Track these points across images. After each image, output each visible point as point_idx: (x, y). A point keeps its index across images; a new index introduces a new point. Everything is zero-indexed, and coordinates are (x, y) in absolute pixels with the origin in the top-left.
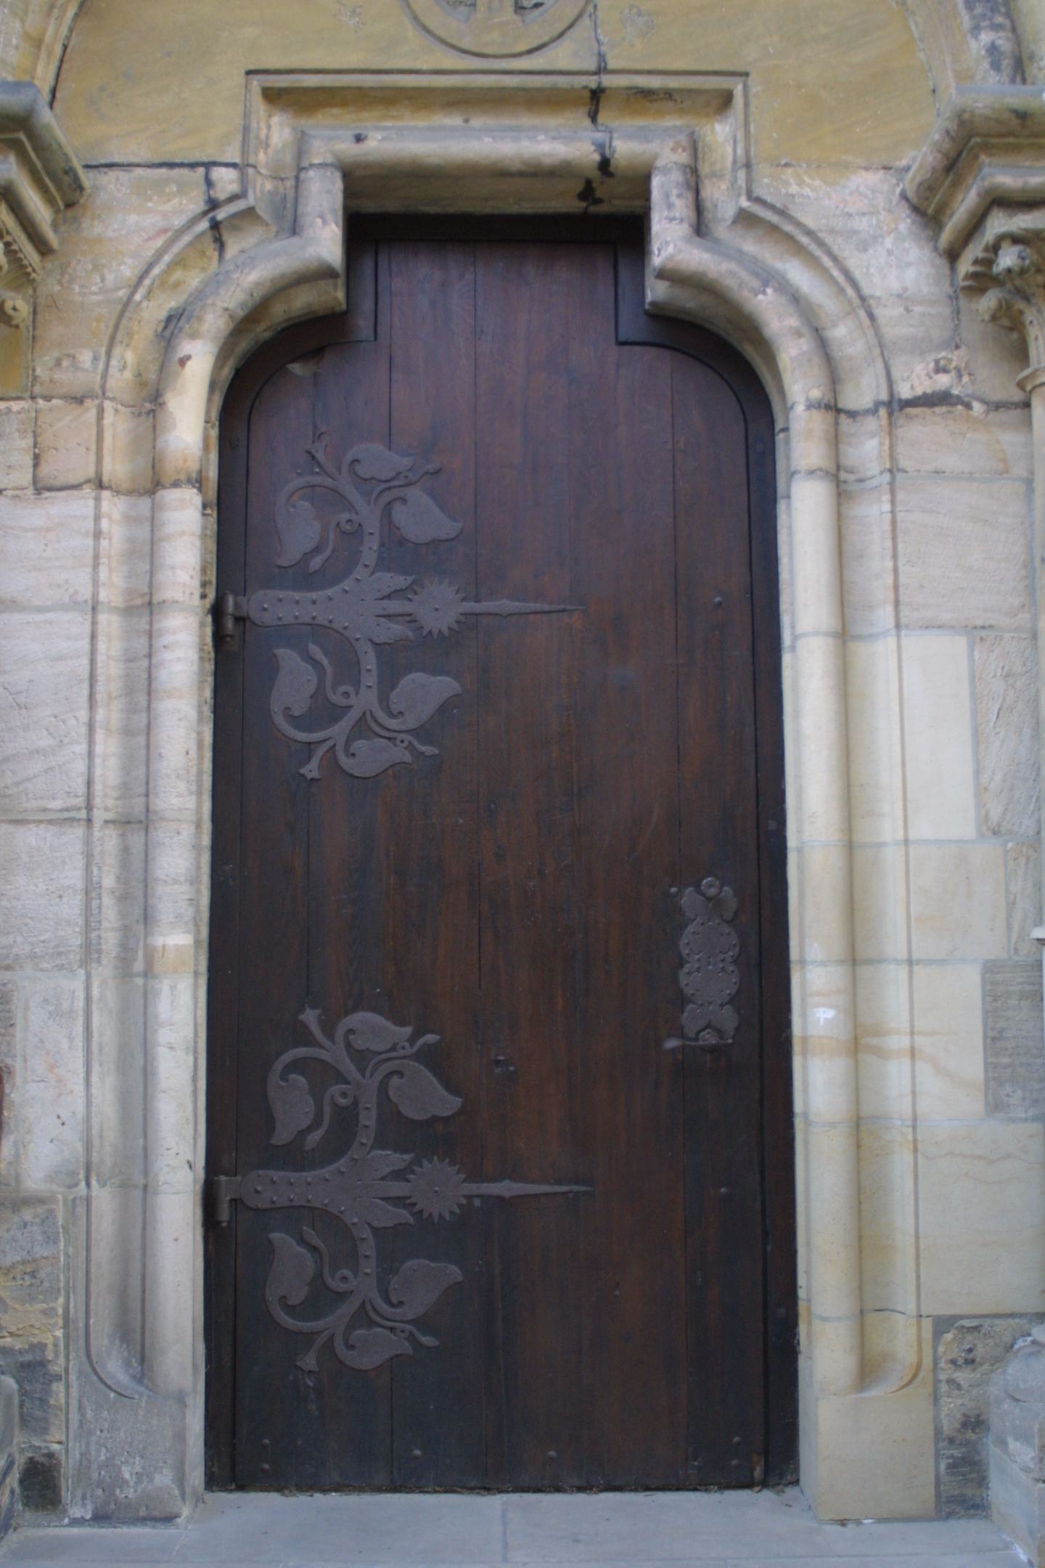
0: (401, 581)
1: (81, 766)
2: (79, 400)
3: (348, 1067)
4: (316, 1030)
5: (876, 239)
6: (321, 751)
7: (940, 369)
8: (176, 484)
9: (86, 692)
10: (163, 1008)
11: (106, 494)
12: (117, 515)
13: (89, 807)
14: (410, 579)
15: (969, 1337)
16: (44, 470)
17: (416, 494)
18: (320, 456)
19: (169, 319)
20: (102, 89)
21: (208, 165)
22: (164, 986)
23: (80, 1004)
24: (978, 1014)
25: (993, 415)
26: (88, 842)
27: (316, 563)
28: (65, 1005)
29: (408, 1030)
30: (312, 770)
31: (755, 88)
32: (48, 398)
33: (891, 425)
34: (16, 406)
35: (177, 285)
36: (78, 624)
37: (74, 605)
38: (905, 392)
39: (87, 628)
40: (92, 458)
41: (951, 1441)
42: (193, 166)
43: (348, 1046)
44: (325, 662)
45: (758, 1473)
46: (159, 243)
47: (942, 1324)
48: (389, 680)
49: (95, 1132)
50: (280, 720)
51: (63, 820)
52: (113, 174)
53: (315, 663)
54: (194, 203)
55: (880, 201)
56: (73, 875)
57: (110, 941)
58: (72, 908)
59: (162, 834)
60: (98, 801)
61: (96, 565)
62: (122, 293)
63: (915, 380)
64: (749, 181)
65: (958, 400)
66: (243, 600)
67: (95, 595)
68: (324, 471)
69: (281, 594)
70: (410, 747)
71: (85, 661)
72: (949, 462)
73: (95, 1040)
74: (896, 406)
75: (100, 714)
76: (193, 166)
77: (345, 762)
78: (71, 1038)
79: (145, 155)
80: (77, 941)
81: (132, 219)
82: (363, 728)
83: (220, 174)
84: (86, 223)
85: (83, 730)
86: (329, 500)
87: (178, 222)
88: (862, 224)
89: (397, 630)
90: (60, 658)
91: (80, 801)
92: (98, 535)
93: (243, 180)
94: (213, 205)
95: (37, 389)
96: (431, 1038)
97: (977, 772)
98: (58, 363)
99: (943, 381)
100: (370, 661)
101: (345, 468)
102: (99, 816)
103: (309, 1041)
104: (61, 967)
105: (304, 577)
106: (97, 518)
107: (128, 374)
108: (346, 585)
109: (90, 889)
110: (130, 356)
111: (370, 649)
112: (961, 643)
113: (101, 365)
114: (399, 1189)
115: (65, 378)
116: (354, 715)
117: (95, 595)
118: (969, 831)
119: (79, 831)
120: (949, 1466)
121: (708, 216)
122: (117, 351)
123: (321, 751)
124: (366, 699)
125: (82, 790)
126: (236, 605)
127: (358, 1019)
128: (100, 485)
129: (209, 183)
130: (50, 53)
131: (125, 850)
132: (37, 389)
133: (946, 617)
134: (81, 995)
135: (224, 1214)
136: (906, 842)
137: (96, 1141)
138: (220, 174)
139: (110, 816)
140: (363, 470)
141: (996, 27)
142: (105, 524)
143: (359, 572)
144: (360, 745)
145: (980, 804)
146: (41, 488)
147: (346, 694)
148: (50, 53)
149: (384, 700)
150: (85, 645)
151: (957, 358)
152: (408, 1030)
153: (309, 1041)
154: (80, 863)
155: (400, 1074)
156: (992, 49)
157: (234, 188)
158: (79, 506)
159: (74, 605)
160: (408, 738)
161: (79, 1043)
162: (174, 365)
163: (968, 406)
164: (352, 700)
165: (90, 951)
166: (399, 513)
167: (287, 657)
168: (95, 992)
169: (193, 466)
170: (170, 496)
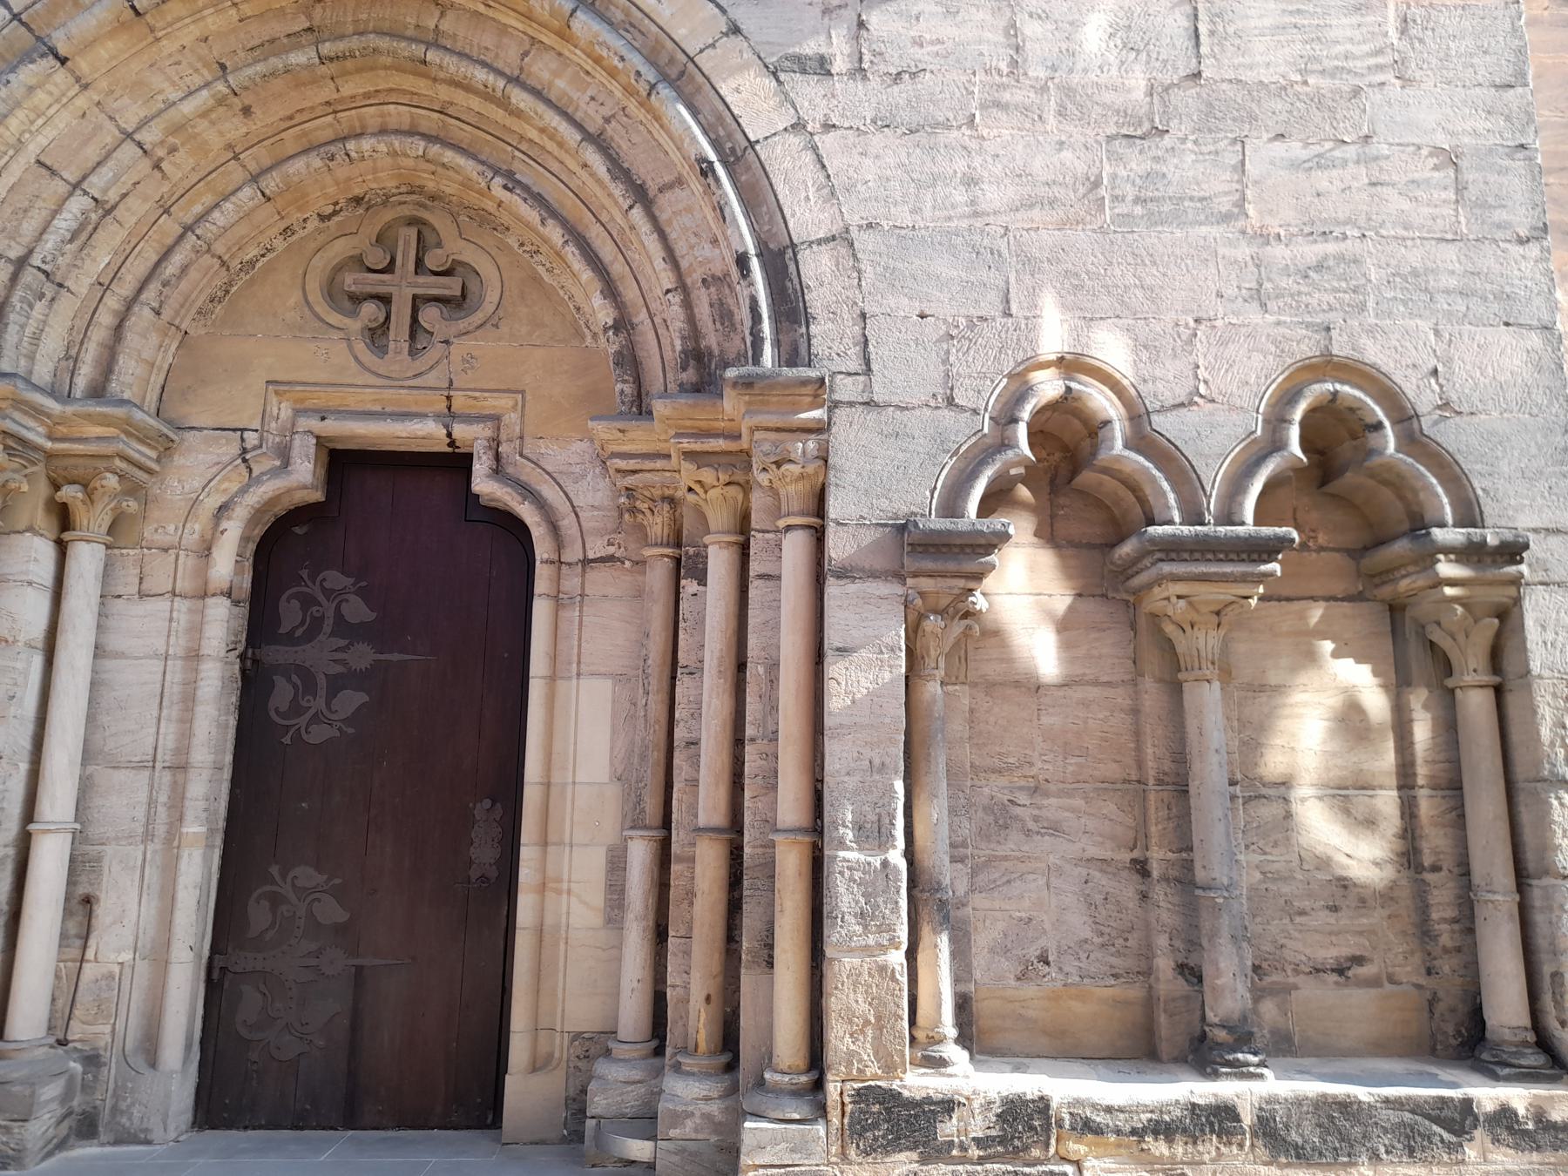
0: (343, 643)
1: (151, 740)
2: (166, 550)
3: (292, 897)
4: (277, 878)
5: (584, 476)
6: (293, 730)
7: (610, 544)
8: (213, 595)
9: (158, 701)
10: (183, 865)
11: (177, 599)
12: (184, 609)
13: (154, 761)
14: (347, 642)
15: (587, 1043)
16: (144, 586)
17: (352, 598)
18: (305, 576)
19: (220, 507)
20: (189, 387)
21: (243, 430)
22: (185, 854)
23: (139, 863)
24: (603, 873)
25: (636, 567)
26: (152, 779)
27: (299, 633)
28: (131, 864)
29: (325, 877)
30: (287, 740)
31: (528, 397)
32: (149, 549)
33: (584, 571)
34: (132, 552)
35: (225, 490)
36: (157, 666)
37: (156, 656)
38: (591, 555)
39: (162, 668)
40: (171, 580)
41: (574, 1100)
42: (234, 430)
43: (293, 885)
44: (299, 682)
45: (489, 1121)
46: (214, 470)
47: (577, 1036)
48: (332, 693)
49: (141, 931)
50: (273, 714)
51: (140, 766)
52: (193, 432)
53: (295, 686)
54: (235, 450)
55: (587, 457)
56: (143, 796)
57: (161, 830)
58: (140, 813)
59: (192, 774)
60: (159, 757)
61: (168, 636)
62: (194, 496)
63: (597, 549)
64: (522, 446)
65: (619, 559)
66: (257, 651)
67: (167, 651)
68: (306, 585)
69: (278, 647)
70: (340, 729)
71: (158, 686)
72: (611, 591)
73: (146, 882)
74: (586, 562)
75: (165, 712)
76: (234, 430)
77: (305, 736)
78: (133, 881)
79: (210, 424)
80: (140, 830)
81: (201, 456)
82: (316, 719)
83: (246, 434)
84: (176, 457)
85: (155, 721)
86: (307, 601)
87: (226, 459)
88: (577, 469)
89: (339, 669)
90: (145, 683)
91: (150, 758)
92: (171, 620)
93: (261, 439)
94: (245, 451)
95: (144, 543)
96: (337, 881)
97: (612, 749)
98: (156, 530)
99: (611, 550)
100: (322, 682)
101: (318, 583)
102: (159, 765)
103: (274, 882)
104: (131, 844)
105: (290, 639)
106: (171, 612)
107: (196, 536)
108: (312, 644)
109: (151, 803)
110: (197, 527)
111: (323, 677)
112: (608, 683)
113: (180, 533)
114: (314, 962)
115: (160, 538)
116: (312, 712)
117: (167, 651)
118: (606, 779)
119: (147, 773)
120: (572, 1114)
121: (504, 461)
122: (188, 525)
123: (293, 730)
124: (319, 703)
125: (151, 751)
126: (253, 653)
127: (297, 871)
128: (174, 595)
129: (243, 440)
130: (160, 369)
131: (175, 782)
132: (144, 543)
133: (602, 670)
134: (140, 858)
135: (216, 975)
136: (574, 783)
137: (141, 935)
138: (246, 434)
139: (167, 764)
140: (327, 585)
141: (624, 382)
142: (175, 615)
143: (321, 637)
144: (314, 728)
145: (612, 764)
146: (142, 595)
147: (309, 701)
148: (160, 369)
149: (328, 704)
150: (160, 677)
151: (619, 538)
152: (325, 877)
153: (274, 882)
154: (146, 788)
155: (319, 900)
156: (622, 391)
157: (256, 442)
158: (162, 605)
159: (156, 656)
160: (339, 724)
161: (137, 883)
162: (218, 534)
163: (623, 563)
164: (312, 704)
165: (148, 836)
166: (345, 609)
167: (280, 681)
168: (149, 856)
169: (226, 586)
170: (210, 601)
